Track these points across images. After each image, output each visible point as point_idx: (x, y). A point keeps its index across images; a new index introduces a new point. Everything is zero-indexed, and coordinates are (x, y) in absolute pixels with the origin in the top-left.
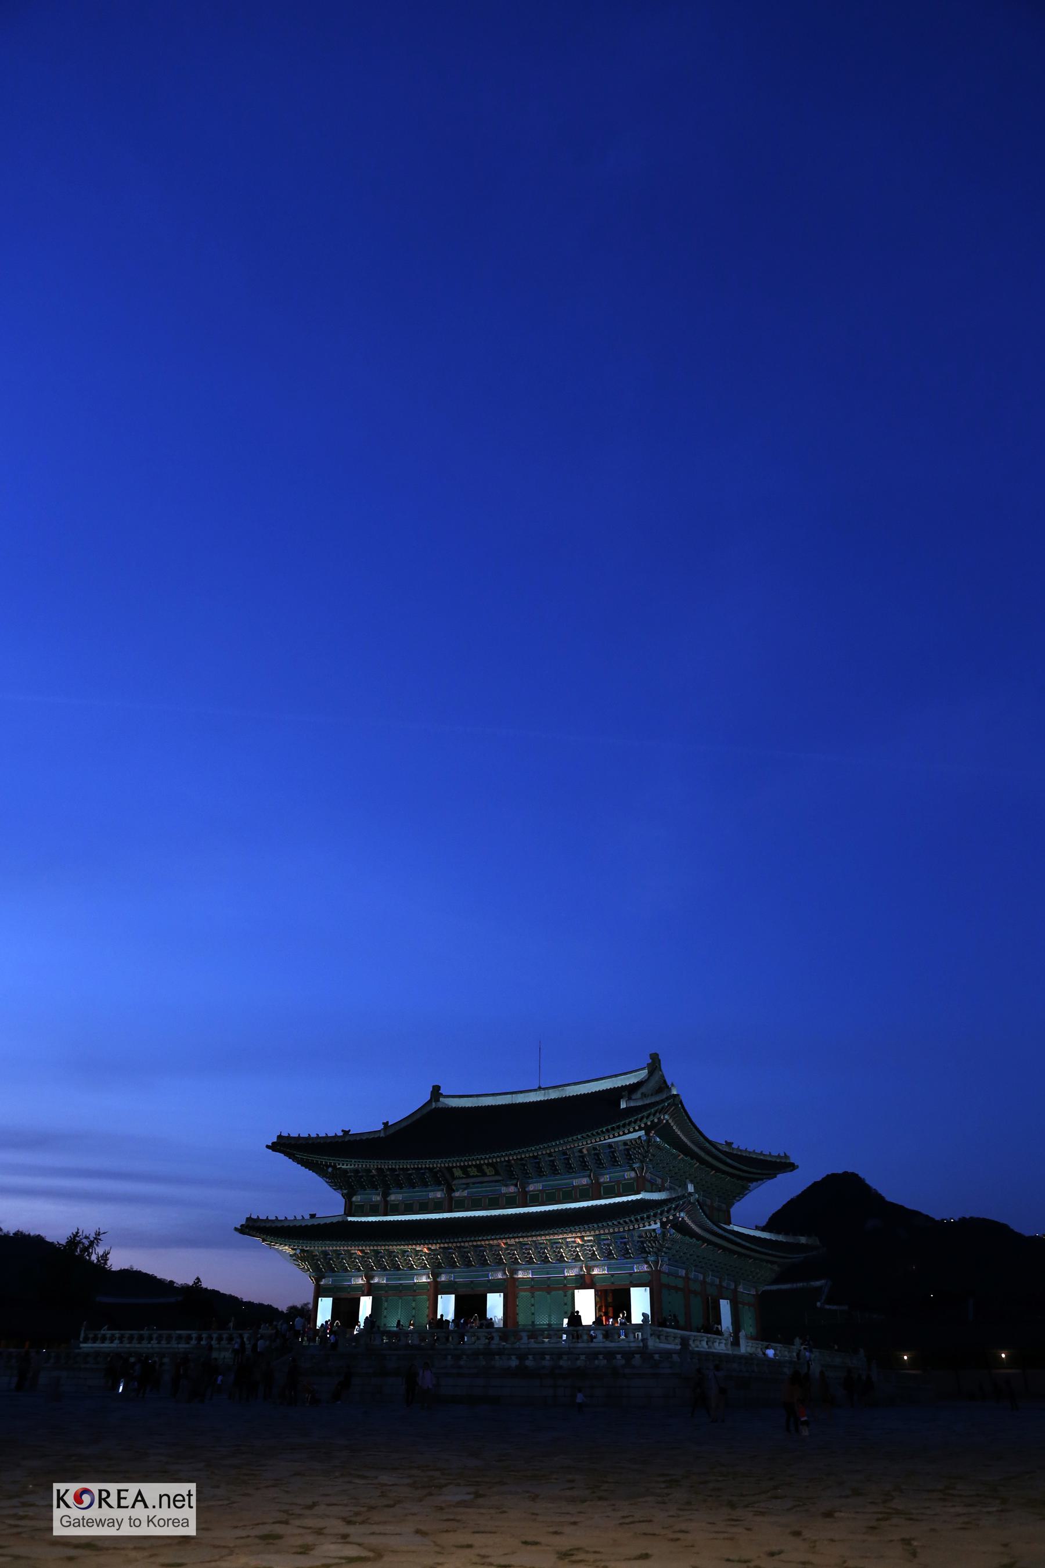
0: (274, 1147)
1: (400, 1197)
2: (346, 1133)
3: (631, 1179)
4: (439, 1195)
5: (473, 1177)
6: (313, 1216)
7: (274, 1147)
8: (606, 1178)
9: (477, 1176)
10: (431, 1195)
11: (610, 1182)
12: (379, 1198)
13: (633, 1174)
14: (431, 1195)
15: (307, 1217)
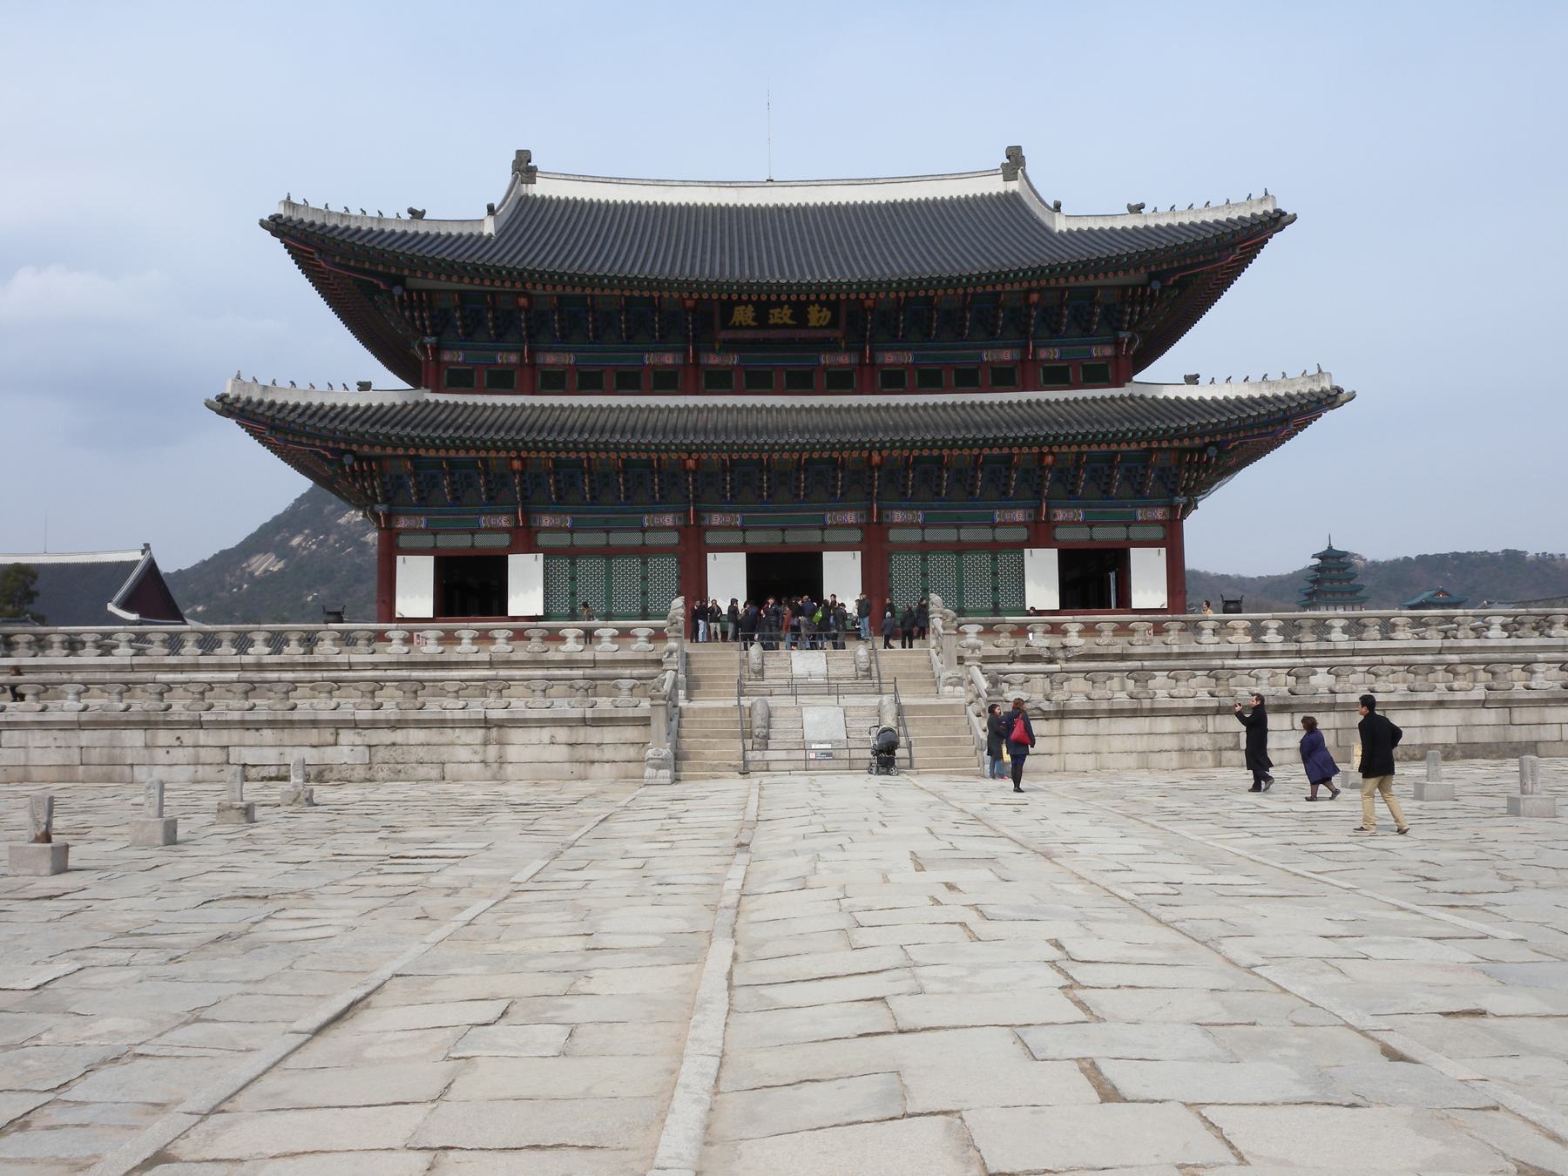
0: (277, 226)
1: (569, 359)
2: (416, 215)
3: (1105, 357)
4: (669, 359)
5: (776, 326)
6: (365, 386)
7: (277, 226)
8: (1049, 354)
9: (785, 326)
10: (650, 359)
11: (1060, 360)
12: (513, 358)
13: (1108, 351)
14: (650, 359)
15: (354, 388)
